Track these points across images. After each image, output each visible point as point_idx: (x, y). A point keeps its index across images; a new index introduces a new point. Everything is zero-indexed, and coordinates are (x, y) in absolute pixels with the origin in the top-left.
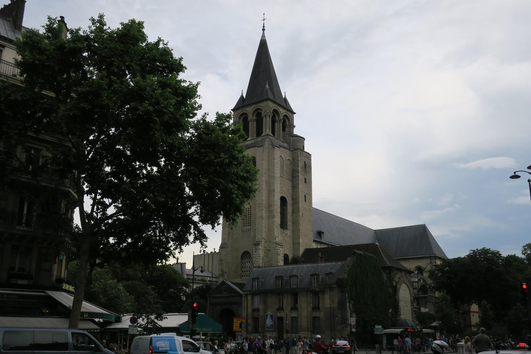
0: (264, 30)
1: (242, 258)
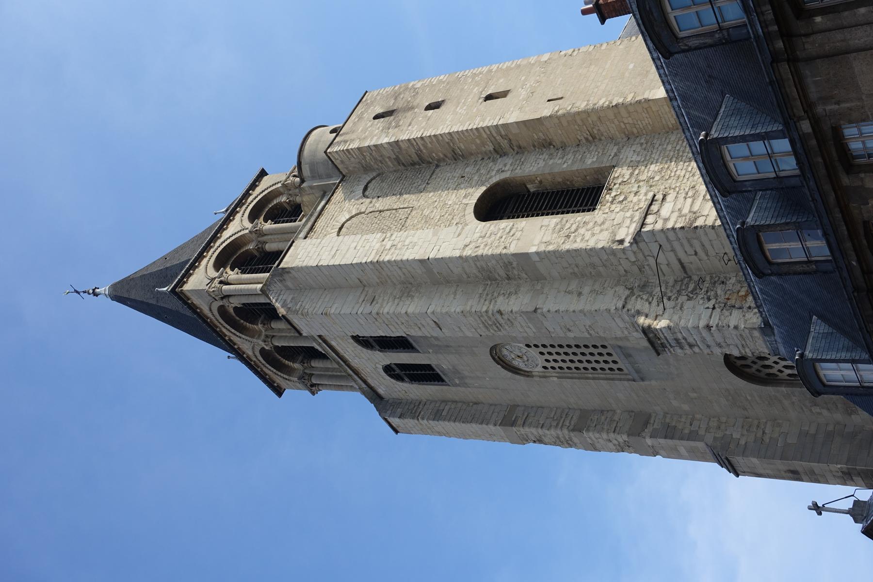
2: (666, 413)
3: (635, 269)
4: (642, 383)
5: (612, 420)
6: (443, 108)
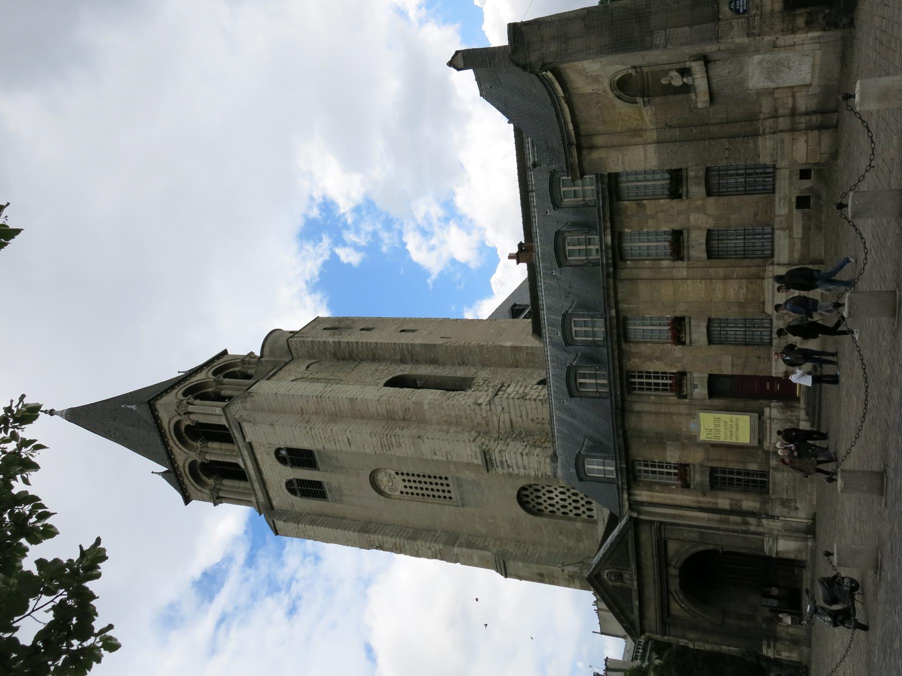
1: (539, 513)
2: (469, 535)
3: (484, 422)
4: (462, 509)
5: (434, 536)
6: (373, 331)
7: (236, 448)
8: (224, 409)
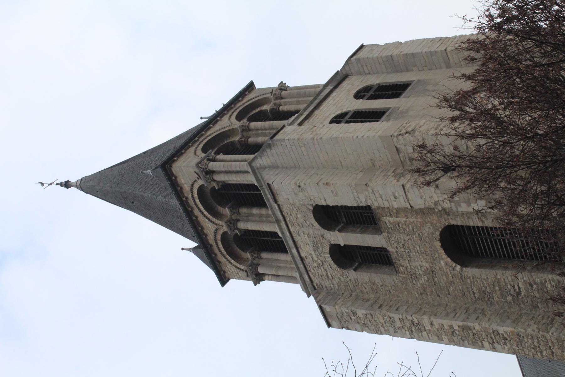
0: (67, 185)
7: (270, 212)
8: (250, 164)
